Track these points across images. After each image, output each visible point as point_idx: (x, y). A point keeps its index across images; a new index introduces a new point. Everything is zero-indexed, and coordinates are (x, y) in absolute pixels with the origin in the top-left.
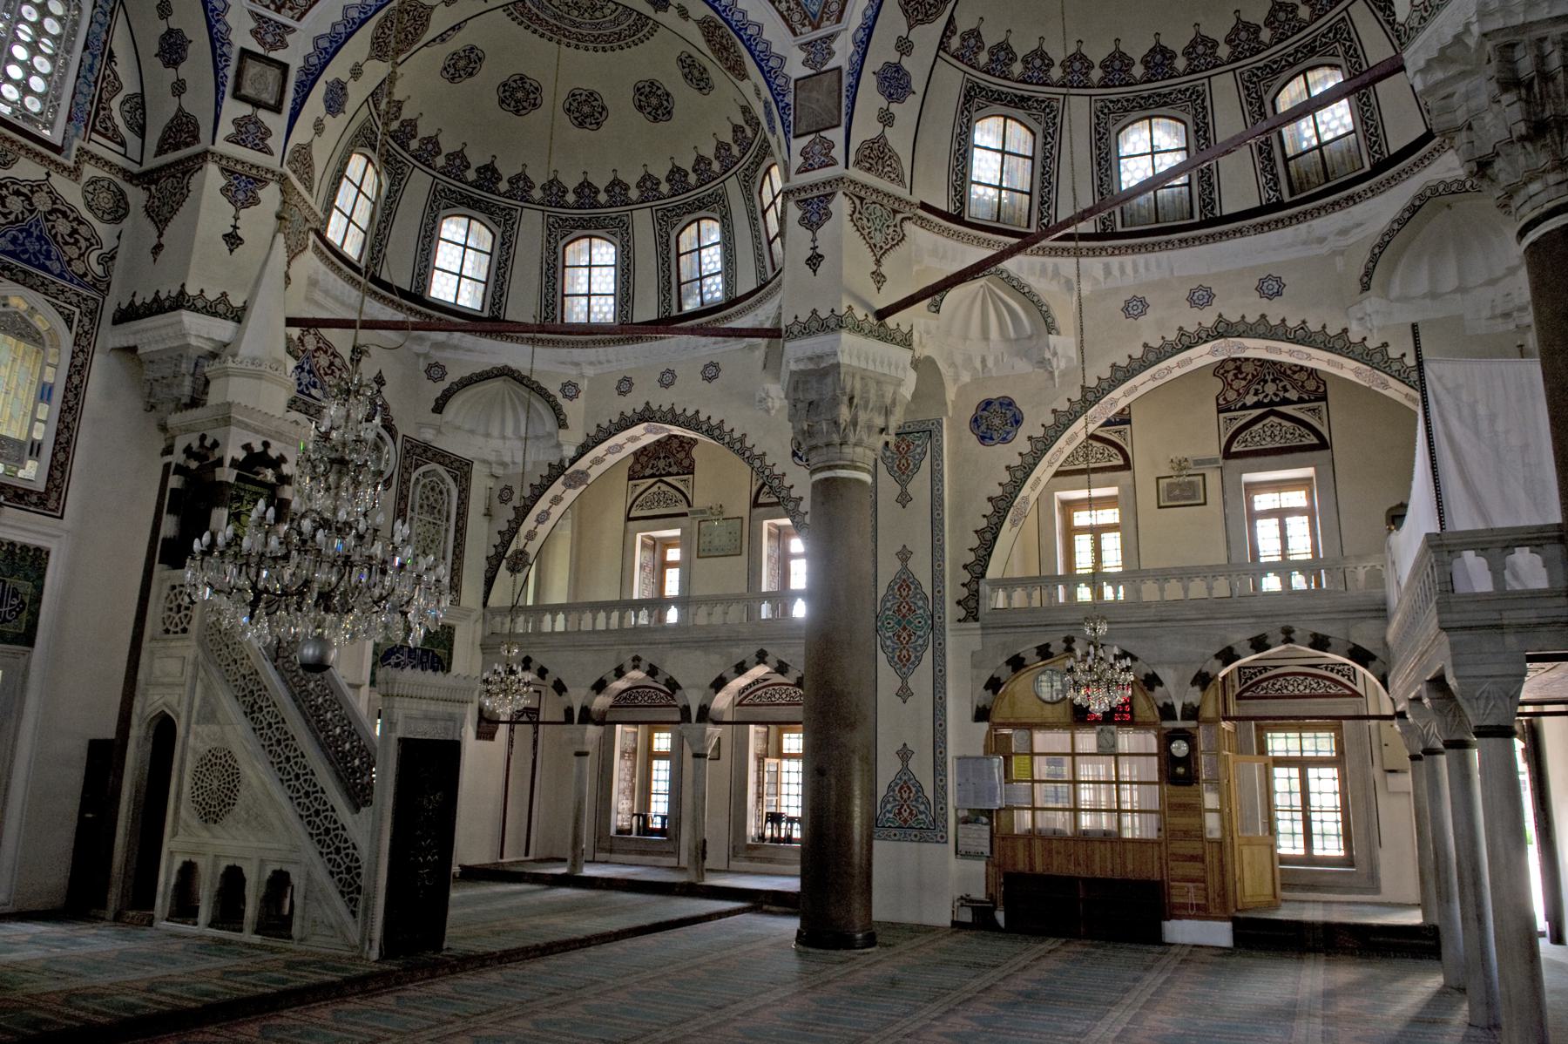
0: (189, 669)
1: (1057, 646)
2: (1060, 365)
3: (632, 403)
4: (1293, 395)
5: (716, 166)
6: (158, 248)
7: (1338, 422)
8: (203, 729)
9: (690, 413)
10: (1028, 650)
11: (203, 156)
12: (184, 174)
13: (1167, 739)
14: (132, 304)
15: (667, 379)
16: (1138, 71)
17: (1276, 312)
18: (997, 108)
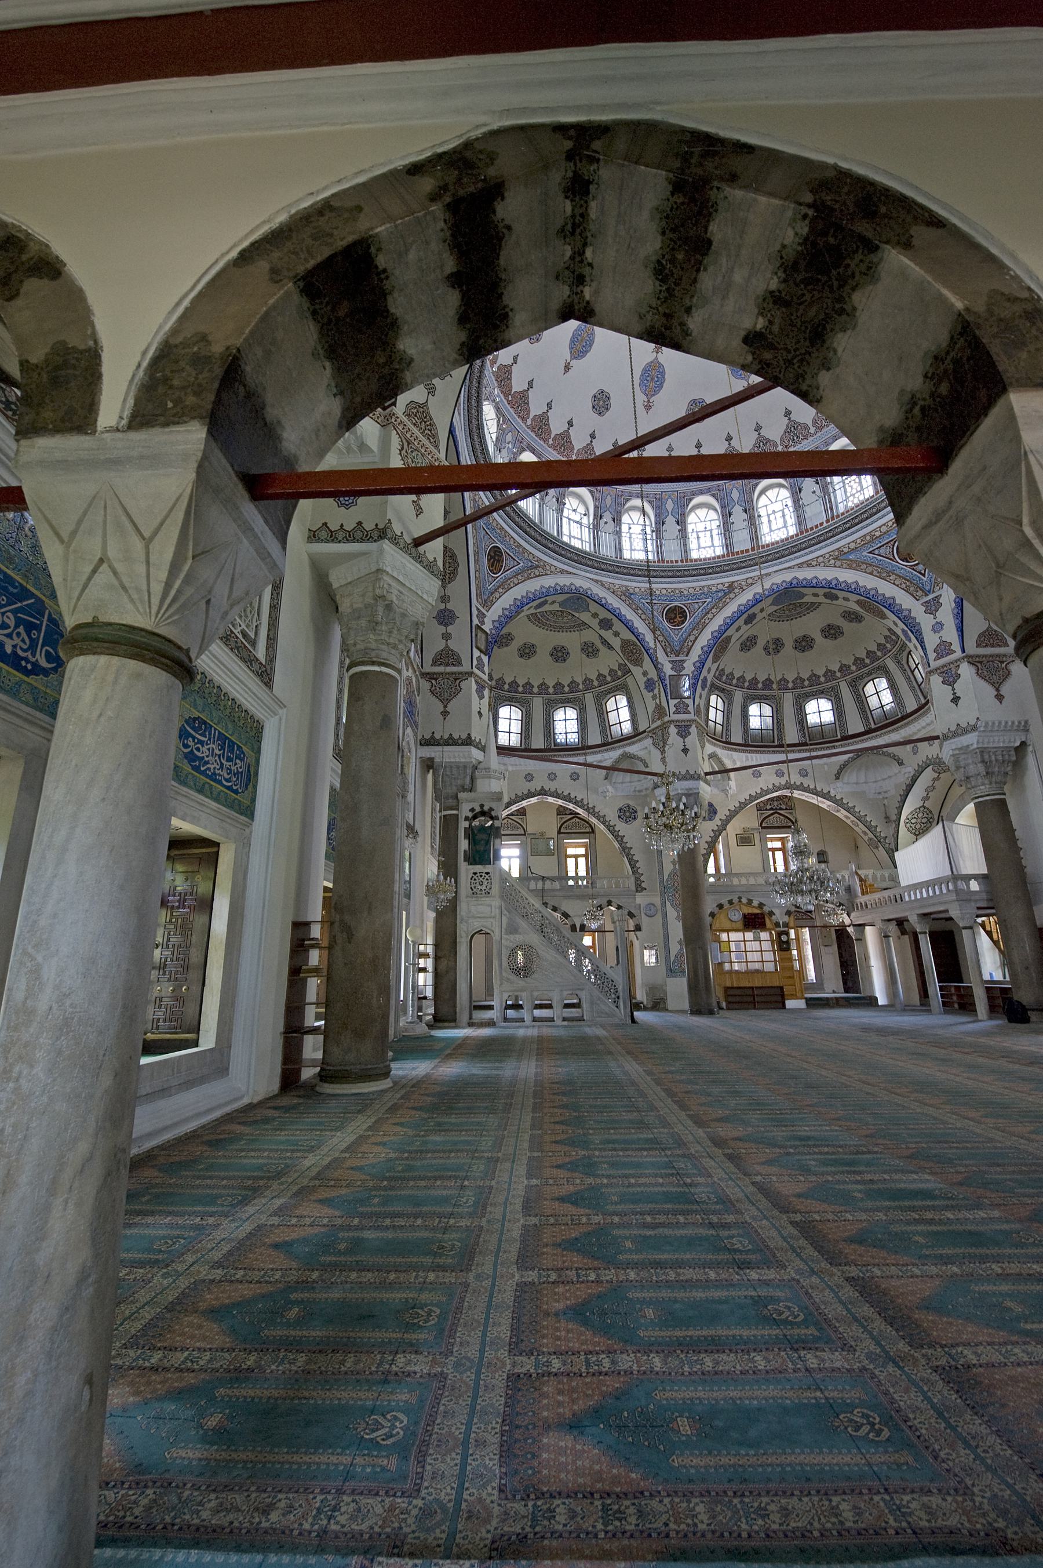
0: (496, 912)
1: (736, 900)
2: (731, 792)
3: (535, 785)
4: (783, 807)
5: (581, 687)
6: (445, 713)
7: (800, 816)
8: (512, 937)
9: (565, 794)
10: (724, 901)
11: (471, 674)
12: (456, 679)
13: (779, 934)
14: (433, 737)
15: (552, 777)
16: (760, 685)
17: (807, 782)
18: (717, 692)
